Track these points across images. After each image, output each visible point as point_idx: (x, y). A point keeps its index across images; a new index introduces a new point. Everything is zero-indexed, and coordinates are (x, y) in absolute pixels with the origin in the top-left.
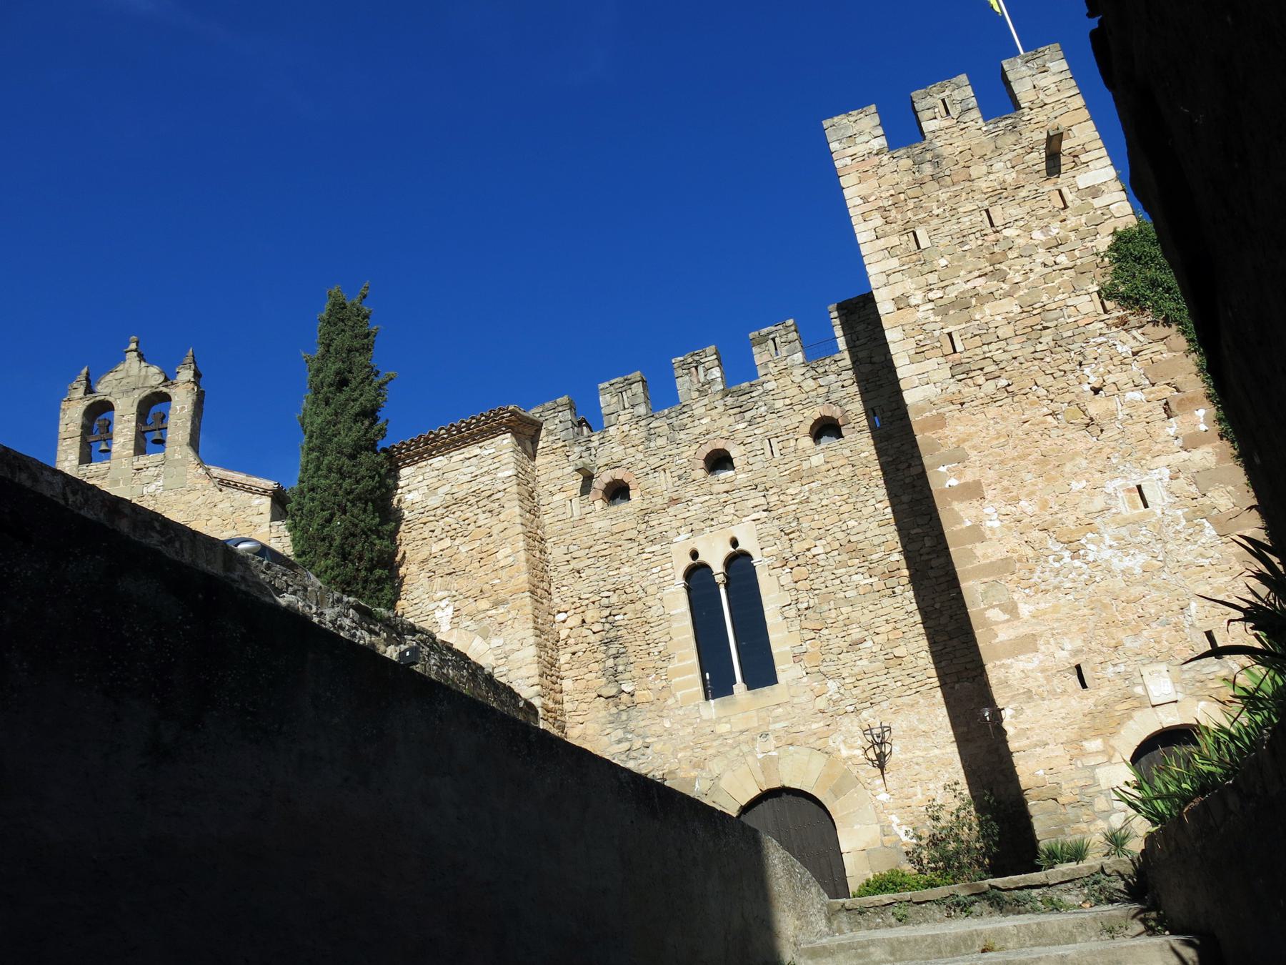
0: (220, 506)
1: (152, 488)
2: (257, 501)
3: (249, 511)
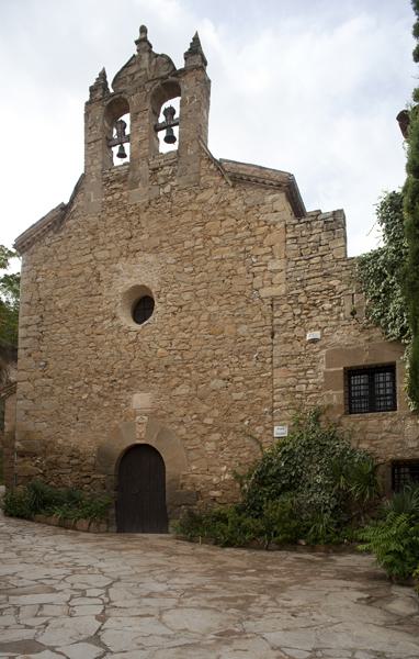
0: (233, 204)
2: (271, 198)
3: (262, 209)
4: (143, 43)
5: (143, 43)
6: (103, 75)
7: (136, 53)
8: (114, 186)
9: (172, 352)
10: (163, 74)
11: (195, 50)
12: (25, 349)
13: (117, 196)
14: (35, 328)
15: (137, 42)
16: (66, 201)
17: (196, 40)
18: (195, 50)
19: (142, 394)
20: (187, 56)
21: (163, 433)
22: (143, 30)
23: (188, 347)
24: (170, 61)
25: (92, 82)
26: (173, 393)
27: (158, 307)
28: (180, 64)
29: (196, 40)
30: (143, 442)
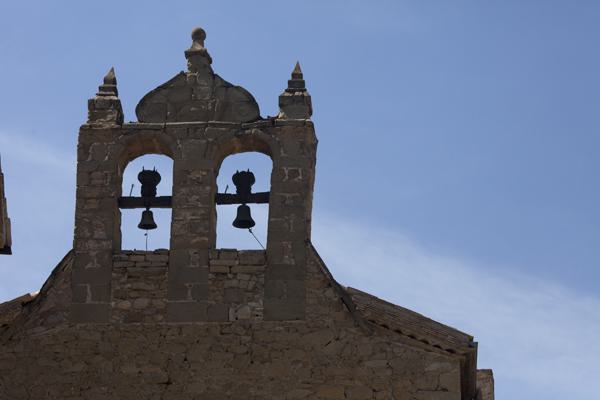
1: (245, 312)
2: (434, 366)
4: (199, 59)
5: (199, 59)
7: (186, 70)
8: (136, 286)
11: (296, 96)
13: (142, 302)
15: (188, 54)
16: (35, 292)
18: (296, 96)
20: (283, 102)
22: (199, 36)
24: (251, 101)
28: (269, 108)
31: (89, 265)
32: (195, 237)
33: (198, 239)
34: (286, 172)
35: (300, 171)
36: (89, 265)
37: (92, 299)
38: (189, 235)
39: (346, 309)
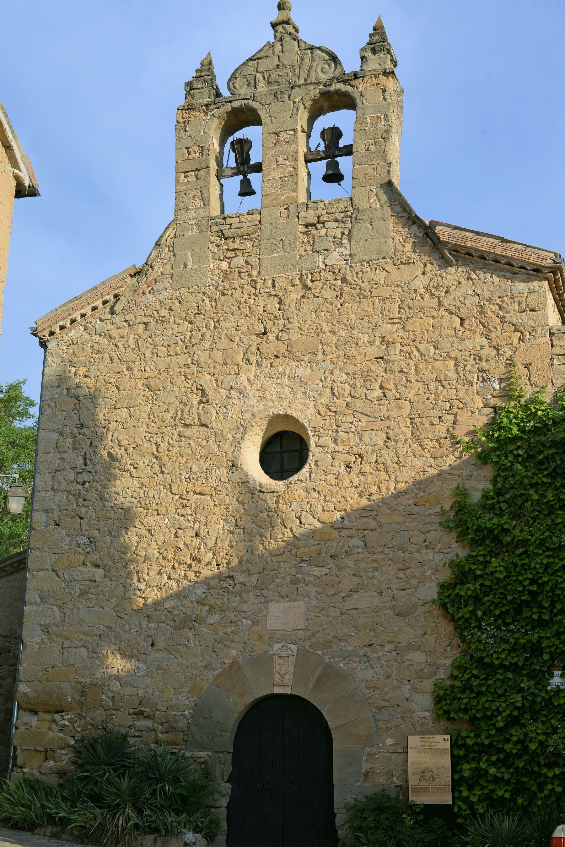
6: (206, 71)
9: (345, 533)
10: (323, 77)
11: (378, 42)
12: (47, 511)
14: (72, 475)
17: (378, 29)
18: (378, 42)
19: (285, 605)
21: (329, 676)
23: (373, 525)
25: (189, 76)
26: (349, 604)
27: (314, 452)
29: (378, 29)
30: (288, 691)
31: (190, 233)
32: (283, 194)
33: (287, 195)
34: (369, 119)
35: (382, 117)
36: (190, 233)
37: (194, 263)
38: (279, 192)
39: (430, 242)
